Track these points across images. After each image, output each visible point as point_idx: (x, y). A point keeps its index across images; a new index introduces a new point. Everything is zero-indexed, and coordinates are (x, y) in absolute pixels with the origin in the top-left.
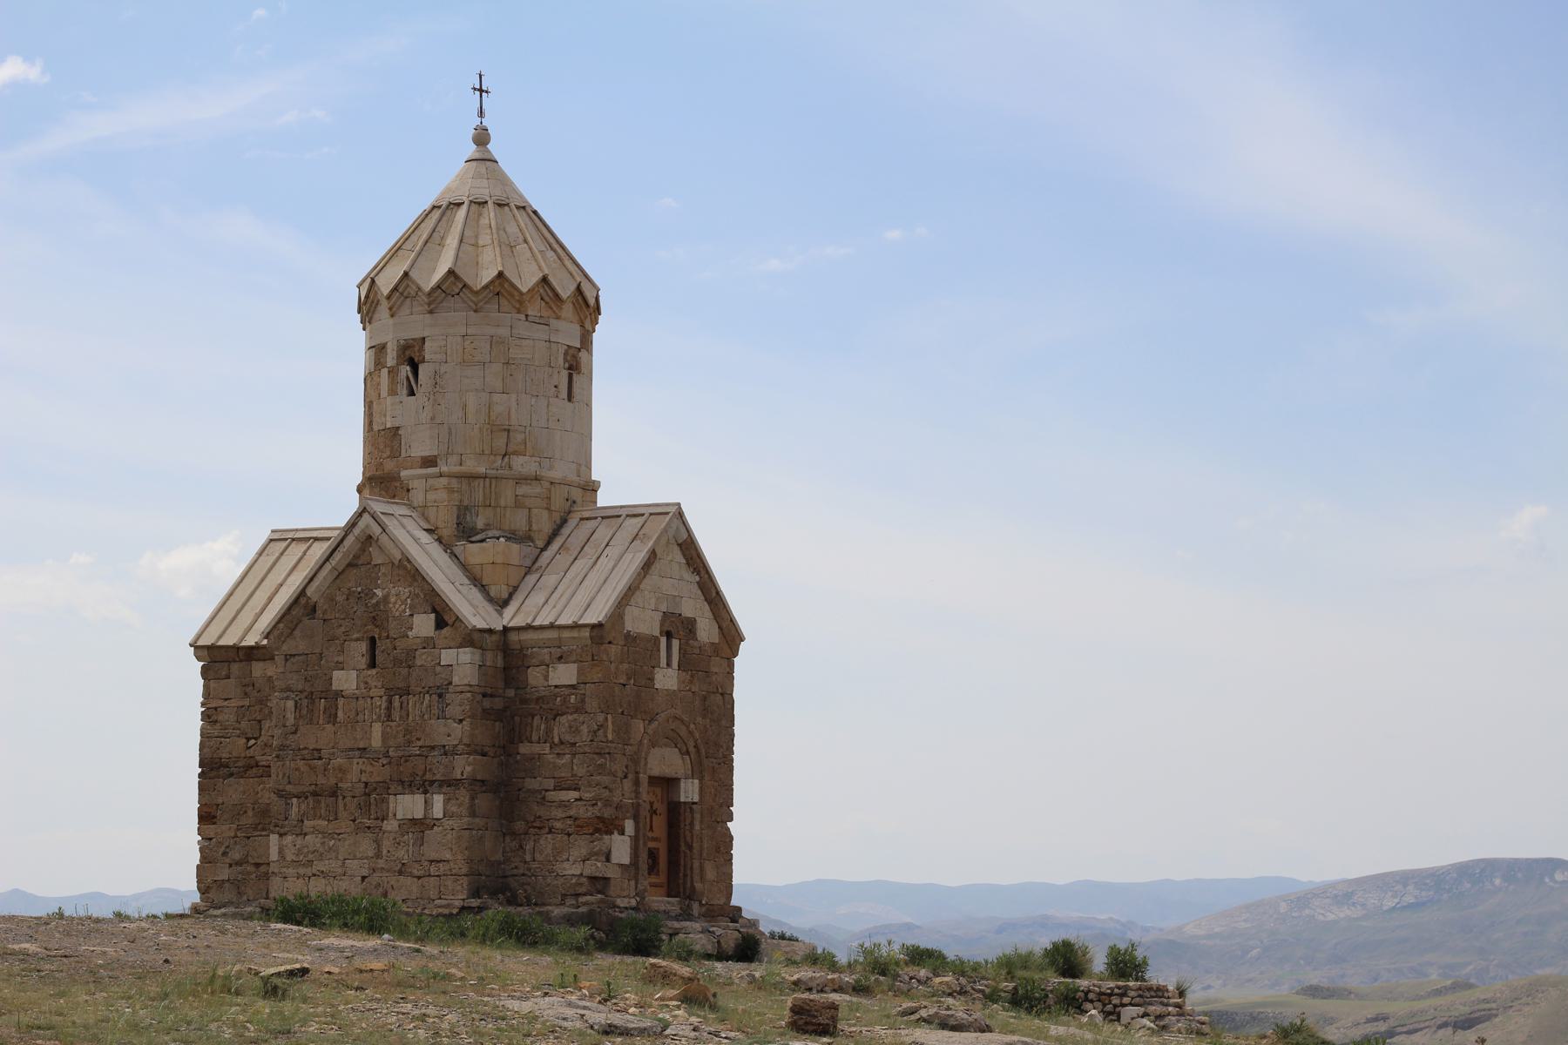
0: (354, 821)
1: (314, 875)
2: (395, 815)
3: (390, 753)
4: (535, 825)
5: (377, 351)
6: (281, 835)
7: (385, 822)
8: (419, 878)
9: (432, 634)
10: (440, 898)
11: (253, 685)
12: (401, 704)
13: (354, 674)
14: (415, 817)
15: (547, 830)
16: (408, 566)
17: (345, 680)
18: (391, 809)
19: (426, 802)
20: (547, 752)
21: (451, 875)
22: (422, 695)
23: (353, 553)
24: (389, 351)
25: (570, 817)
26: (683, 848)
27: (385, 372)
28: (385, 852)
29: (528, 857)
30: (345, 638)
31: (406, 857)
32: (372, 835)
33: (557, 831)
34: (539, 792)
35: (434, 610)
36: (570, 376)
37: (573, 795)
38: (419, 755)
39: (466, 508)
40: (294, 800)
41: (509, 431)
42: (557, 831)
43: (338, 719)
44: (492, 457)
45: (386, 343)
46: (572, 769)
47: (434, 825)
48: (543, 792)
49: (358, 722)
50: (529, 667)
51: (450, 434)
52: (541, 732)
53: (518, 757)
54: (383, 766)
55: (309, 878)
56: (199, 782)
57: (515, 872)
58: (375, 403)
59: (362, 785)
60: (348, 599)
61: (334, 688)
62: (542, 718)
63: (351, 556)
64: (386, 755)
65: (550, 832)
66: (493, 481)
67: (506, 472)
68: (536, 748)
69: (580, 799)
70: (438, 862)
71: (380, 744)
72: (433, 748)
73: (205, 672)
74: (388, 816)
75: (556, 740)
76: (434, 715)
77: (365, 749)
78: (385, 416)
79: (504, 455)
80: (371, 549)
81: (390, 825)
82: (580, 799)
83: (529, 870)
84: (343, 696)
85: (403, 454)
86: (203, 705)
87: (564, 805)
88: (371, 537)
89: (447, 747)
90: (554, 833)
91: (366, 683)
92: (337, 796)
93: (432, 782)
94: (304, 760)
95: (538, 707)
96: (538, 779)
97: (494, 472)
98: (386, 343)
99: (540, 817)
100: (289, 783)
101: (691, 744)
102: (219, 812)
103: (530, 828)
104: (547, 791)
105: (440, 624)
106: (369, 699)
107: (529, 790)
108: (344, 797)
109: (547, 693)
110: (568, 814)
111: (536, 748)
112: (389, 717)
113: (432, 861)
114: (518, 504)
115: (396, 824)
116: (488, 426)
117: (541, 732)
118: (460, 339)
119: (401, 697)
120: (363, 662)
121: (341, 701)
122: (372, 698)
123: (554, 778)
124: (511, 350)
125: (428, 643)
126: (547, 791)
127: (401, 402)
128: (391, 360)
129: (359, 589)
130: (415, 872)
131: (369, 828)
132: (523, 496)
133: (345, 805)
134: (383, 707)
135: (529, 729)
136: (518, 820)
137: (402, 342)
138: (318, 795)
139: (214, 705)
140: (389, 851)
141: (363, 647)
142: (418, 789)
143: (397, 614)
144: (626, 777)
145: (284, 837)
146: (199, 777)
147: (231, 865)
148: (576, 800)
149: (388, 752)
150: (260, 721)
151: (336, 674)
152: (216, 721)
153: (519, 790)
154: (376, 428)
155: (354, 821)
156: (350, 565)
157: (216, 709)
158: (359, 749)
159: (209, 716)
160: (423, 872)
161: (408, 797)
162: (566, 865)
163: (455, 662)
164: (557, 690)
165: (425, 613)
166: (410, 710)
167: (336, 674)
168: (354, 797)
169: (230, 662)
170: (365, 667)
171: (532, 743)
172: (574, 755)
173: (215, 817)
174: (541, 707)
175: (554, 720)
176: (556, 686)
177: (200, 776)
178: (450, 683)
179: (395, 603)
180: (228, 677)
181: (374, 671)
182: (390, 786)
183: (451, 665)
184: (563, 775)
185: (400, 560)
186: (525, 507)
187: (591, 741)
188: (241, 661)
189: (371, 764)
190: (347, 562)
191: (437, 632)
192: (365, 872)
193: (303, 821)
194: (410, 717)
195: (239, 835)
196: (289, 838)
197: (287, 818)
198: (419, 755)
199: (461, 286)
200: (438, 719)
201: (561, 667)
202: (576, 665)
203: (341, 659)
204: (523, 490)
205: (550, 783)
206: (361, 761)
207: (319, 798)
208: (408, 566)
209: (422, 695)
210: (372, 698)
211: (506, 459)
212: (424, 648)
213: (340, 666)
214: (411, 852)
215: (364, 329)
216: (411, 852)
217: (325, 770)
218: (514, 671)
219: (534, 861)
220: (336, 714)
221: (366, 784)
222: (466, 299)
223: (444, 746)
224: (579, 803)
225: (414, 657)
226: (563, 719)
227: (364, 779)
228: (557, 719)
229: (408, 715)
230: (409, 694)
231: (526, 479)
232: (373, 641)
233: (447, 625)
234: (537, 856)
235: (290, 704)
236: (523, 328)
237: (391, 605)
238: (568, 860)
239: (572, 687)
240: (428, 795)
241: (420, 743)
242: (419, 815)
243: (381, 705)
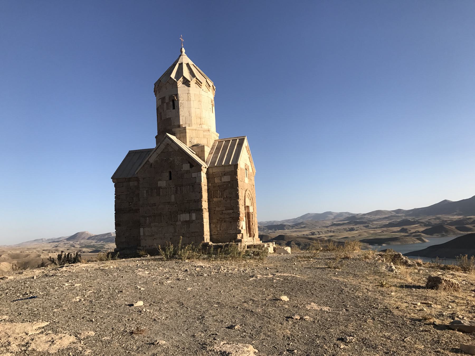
0: (167, 223)
1: (155, 239)
2: (180, 220)
3: (178, 203)
4: (220, 220)
5: (163, 99)
6: (144, 228)
7: (177, 222)
8: (189, 237)
9: (189, 169)
10: (196, 243)
11: (130, 188)
12: (180, 189)
13: (165, 182)
14: (187, 220)
15: (224, 221)
16: (181, 151)
17: (162, 184)
18: (178, 219)
19: (190, 216)
20: (222, 200)
21: (199, 236)
22: (187, 186)
23: (163, 149)
24: (166, 99)
25: (231, 217)
26: (251, 224)
27: (165, 104)
28: (177, 231)
29: (218, 229)
30: (161, 172)
31: (184, 232)
32: (172, 226)
33: (227, 221)
34: (221, 211)
35: (189, 163)
36: (212, 106)
37: (231, 211)
38: (187, 203)
39: (192, 138)
40: (148, 218)
41: (201, 118)
42: (227, 221)
43: (160, 195)
44: (197, 125)
45: (165, 97)
46: (231, 204)
47: (193, 222)
48: (222, 211)
49: (167, 195)
50: (215, 178)
51: (186, 119)
52: (220, 195)
53: (214, 202)
54: (175, 206)
55: (153, 240)
56: (115, 215)
57: (214, 234)
58: (162, 113)
59: (170, 212)
60: (162, 162)
61: (158, 186)
62: (220, 191)
63: (162, 150)
64: (177, 203)
65: (225, 222)
66: (198, 131)
67: (201, 129)
68: (219, 199)
69: (234, 212)
70: (194, 232)
71: (174, 200)
72: (191, 200)
73: (115, 186)
74: (178, 220)
75: (225, 197)
76: (191, 191)
77: (169, 202)
78: (166, 115)
79: (200, 124)
80: (168, 148)
81: (179, 223)
82: (234, 212)
83: (219, 233)
84: (162, 188)
85: (172, 125)
86: (115, 194)
87: (229, 214)
88: (168, 144)
89: (196, 200)
90: (226, 222)
91: (169, 184)
92: (161, 216)
93: (191, 210)
94: (150, 206)
95: (219, 188)
96: (220, 207)
97: (198, 128)
98: (165, 97)
99: (221, 218)
100: (146, 213)
101: (251, 197)
102: (121, 223)
103: (218, 221)
104: (223, 210)
105: (191, 166)
106: (170, 189)
107: (218, 211)
108: (163, 216)
109: (221, 184)
110: (230, 217)
111: (219, 199)
112: (176, 192)
113: (193, 232)
114: (204, 137)
115: (180, 222)
116: (195, 117)
117: (220, 195)
118: (187, 94)
119: (180, 187)
120: (168, 178)
121: (161, 190)
122: (171, 188)
123: (225, 207)
124: (200, 98)
125: (187, 172)
126: (223, 210)
127: (171, 111)
128: (167, 100)
129: (165, 159)
130: (188, 236)
131: (172, 224)
132: (205, 135)
133: (164, 218)
134: (174, 190)
135: (216, 194)
136: (215, 219)
137: (170, 96)
138: (155, 216)
139: (119, 195)
140: (179, 230)
141: (168, 174)
142: (187, 212)
143: (178, 164)
144: (243, 206)
145: (144, 229)
146: (115, 214)
147: (125, 238)
148: (233, 212)
149: (177, 202)
150: (133, 198)
151: (159, 182)
152: (120, 199)
153: (214, 211)
154: (163, 119)
155: (167, 223)
156: (162, 152)
157: (119, 195)
158: (167, 202)
159: (117, 197)
160: (190, 235)
161: (184, 215)
162: (231, 231)
163: (197, 176)
164: (224, 183)
165: (186, 163)
166: (183, 190)
167: (159, 182)
168: (166, 216)
169: (123, 182)
170: (168, 180)
171: (217, 198)
172: (231, 200)
173: (120, 224)
174: (220, 188)
175: (224, 191)
176: (224, 182)
177: (115, 213)
178: (196, 182)
179: (177, 162)
180: (123, 187)
181: (171, 181)
182: (178, 212)
183: (196, 177)
184: (228, 206)
185: (178, 150)
186: (206, 138)
187: (236, 196)
188: (126, 182)
189: (172, 206)
190: (161, 151)
191: (191, 169)
192: (171, 237)
193: (150, 224)
194: (183, 193)
195: (128, 229)
196: (146, 229)
197: (145, 223)
198: (187, 203)
199: (186, 81)
200: (192, 192)
201: (225, 177)
202: (230, 176)
203: (160, 178)
204: (205, 133)
205: (224, 209)
206: (168, 206)
207: (155, 217)
208: (181, 151)
209: (187, 186)
210: (171, 188)
211: (201, 125)
212: (187, 173)
213: (160, 180)
214: (186, 230)
215: (156, 96)
216: (186, 230)
217: (157, 209)
218: (211, 179)
219: (220, 230)
220: (160, 193)
221: (170, 212)
222: (187, 84)
223: (195, 200)
224: (233, 213)
225: (184, 176)
226: (227, 191)
227: (169, 211)
228: (225, 191)
229: (183, 192)
230: (183, 186)
231: (206, 131)
232: (170, 172)
233: (194, 166)
234: (221, 229)
235: (145, 192)
236: (203, 93)
237: (176, 162)
238: (231, 229)
239: (229, 182)
240: (190, 214)
241: (186, 199)
242: (188, 219)
243: (174, 190)
